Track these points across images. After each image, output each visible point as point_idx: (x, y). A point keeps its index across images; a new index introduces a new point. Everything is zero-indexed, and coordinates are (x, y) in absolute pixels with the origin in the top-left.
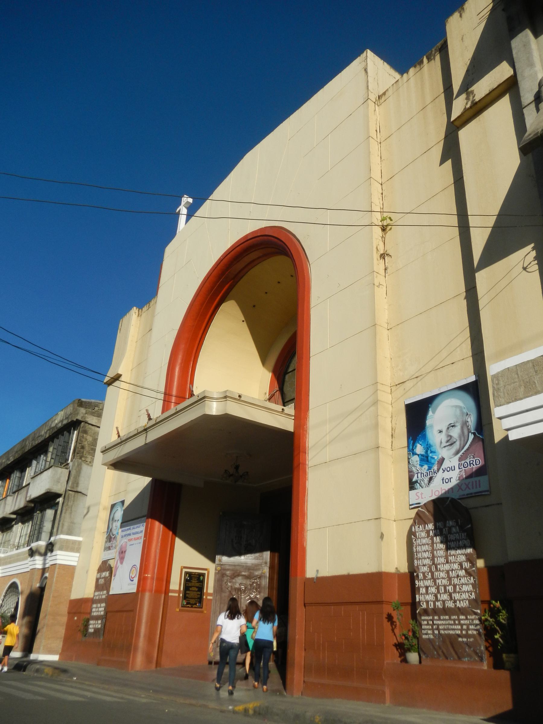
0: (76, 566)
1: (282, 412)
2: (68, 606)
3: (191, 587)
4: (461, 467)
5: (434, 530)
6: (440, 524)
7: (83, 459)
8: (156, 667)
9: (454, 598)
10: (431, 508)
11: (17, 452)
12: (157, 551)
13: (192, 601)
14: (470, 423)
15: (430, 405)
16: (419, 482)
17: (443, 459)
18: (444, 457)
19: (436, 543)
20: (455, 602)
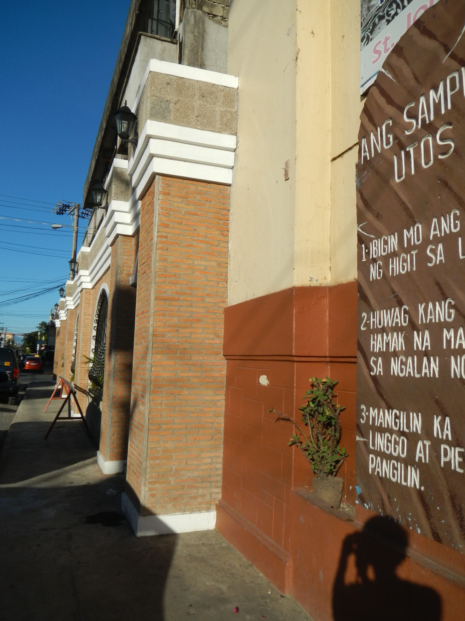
0: (229, 185)
2: (221, 331)
7: (206, 9)
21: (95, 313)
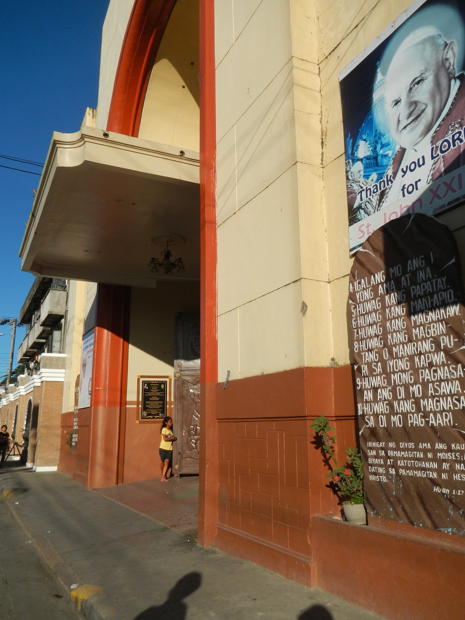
1: (180, 155)
2: (60, 420)
3: (151, 397)
4: (435, 155)
5: (386, 282)
6: (395, 270)
8: (117, 484)
9: (425, 407)
10: (380, 245)
11: (37, 283)
12: (107, 361)
13: (153, 412)
14: (451, 61)
15: (378, 63)
16: (363, 207)
17: (403, 151)
18: (405, 147)
19: (390, 307)
20: (426, 415)
21: (27, 408)
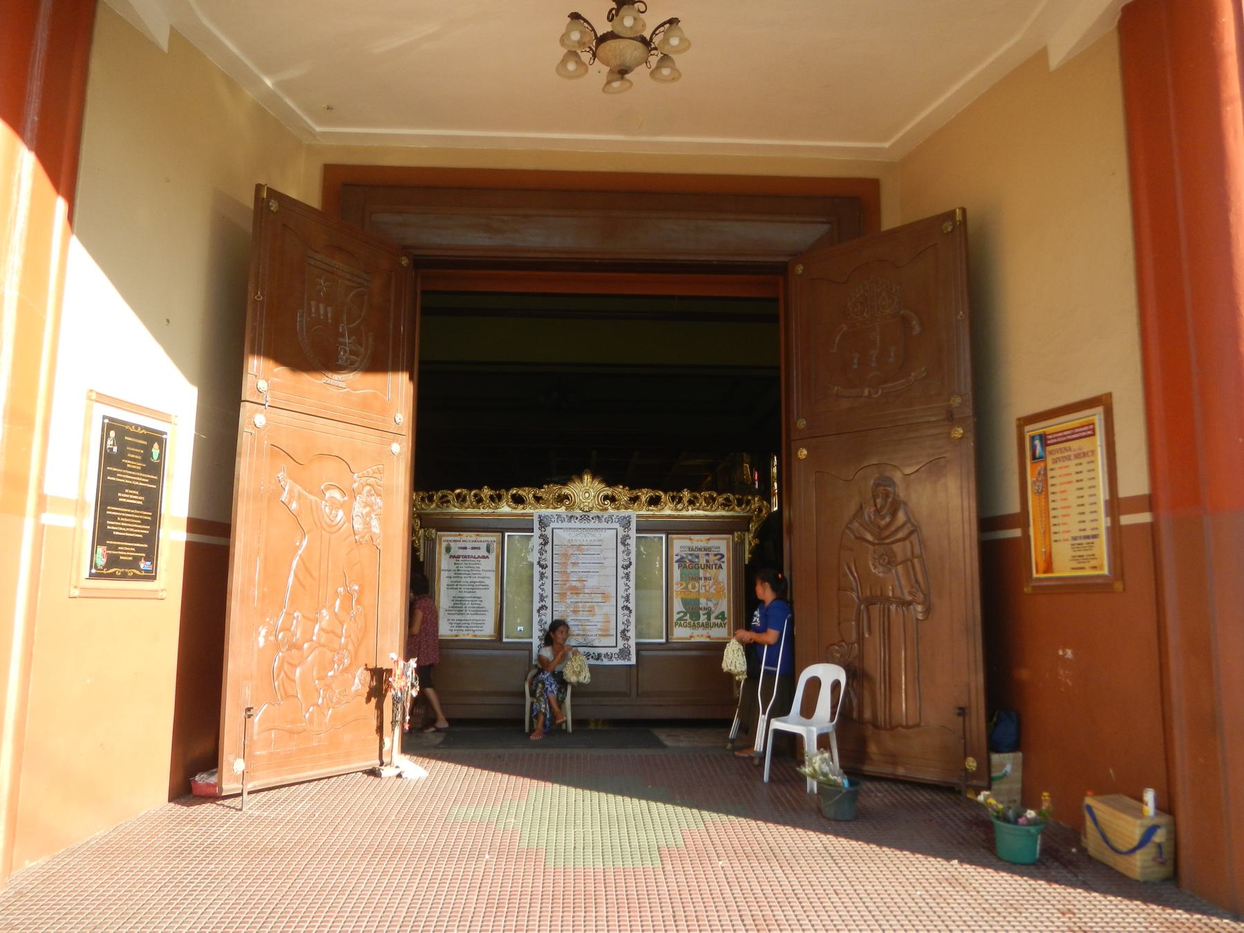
3: (122, 487)
13: (126, 552)
